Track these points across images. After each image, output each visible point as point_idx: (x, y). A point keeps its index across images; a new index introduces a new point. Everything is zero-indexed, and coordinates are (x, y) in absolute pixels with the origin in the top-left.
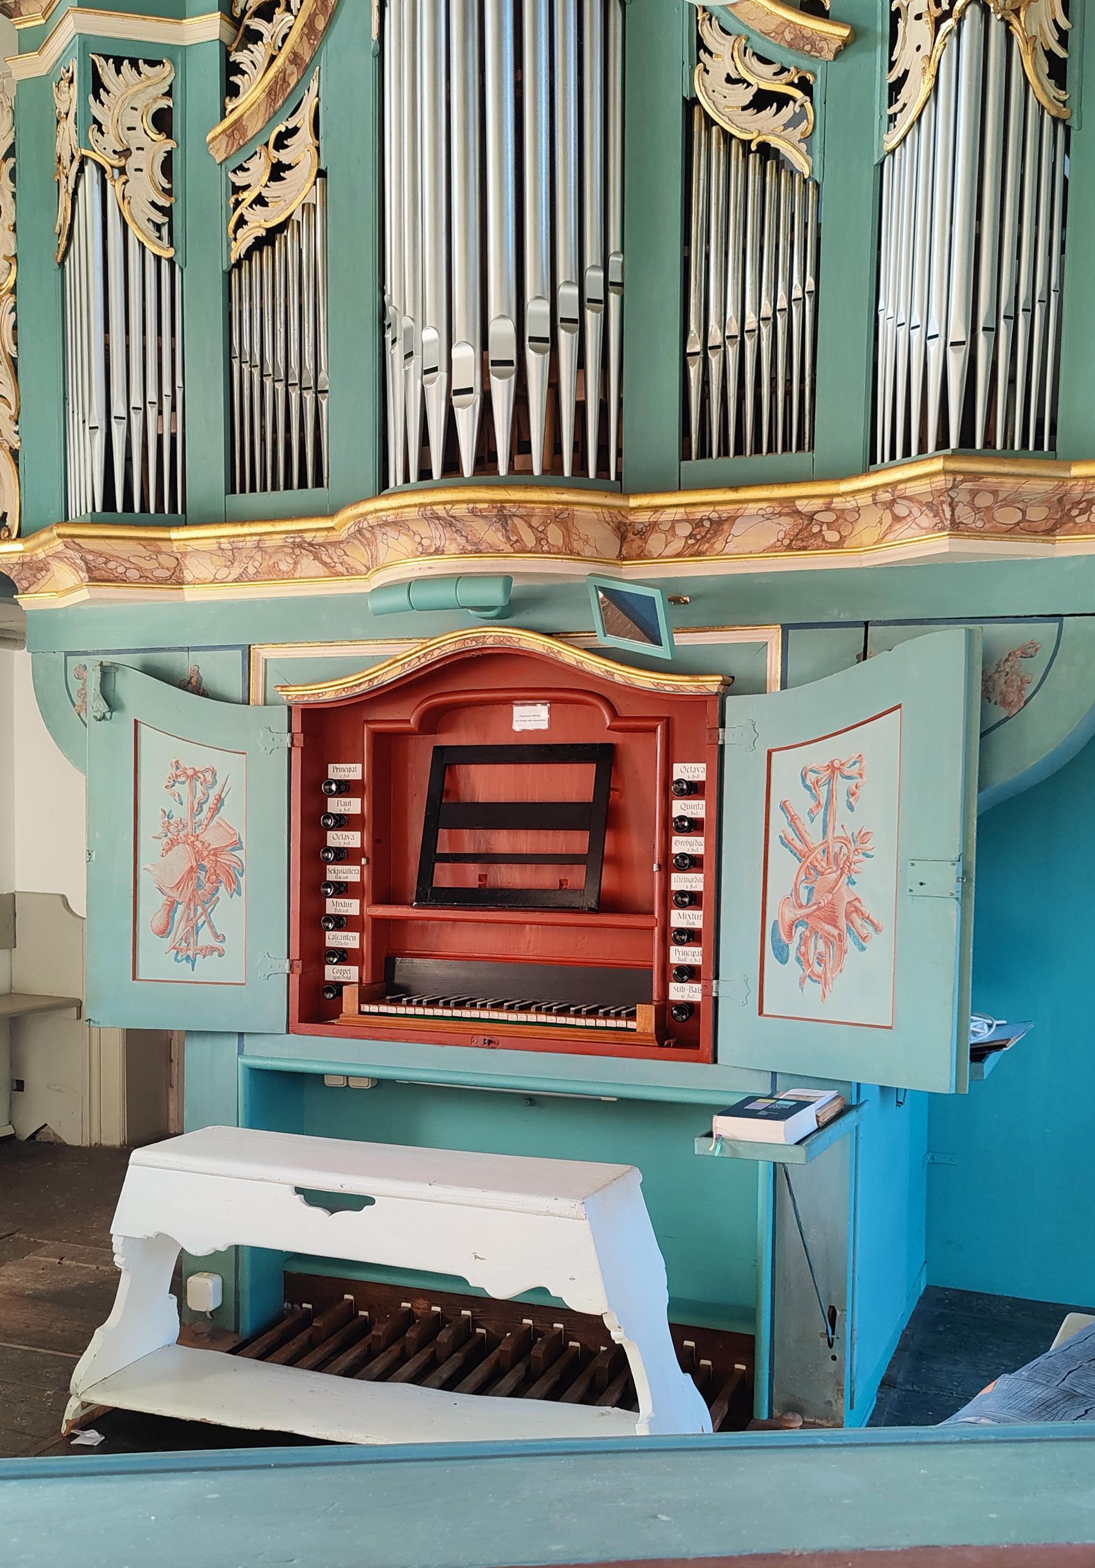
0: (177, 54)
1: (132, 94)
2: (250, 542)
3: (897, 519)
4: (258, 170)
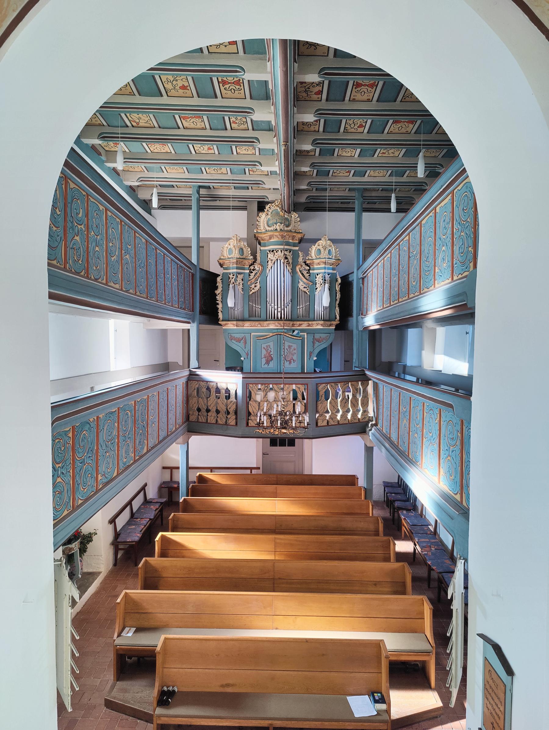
0: (244, 273)
1: (240, 277)
4: (253, 286)
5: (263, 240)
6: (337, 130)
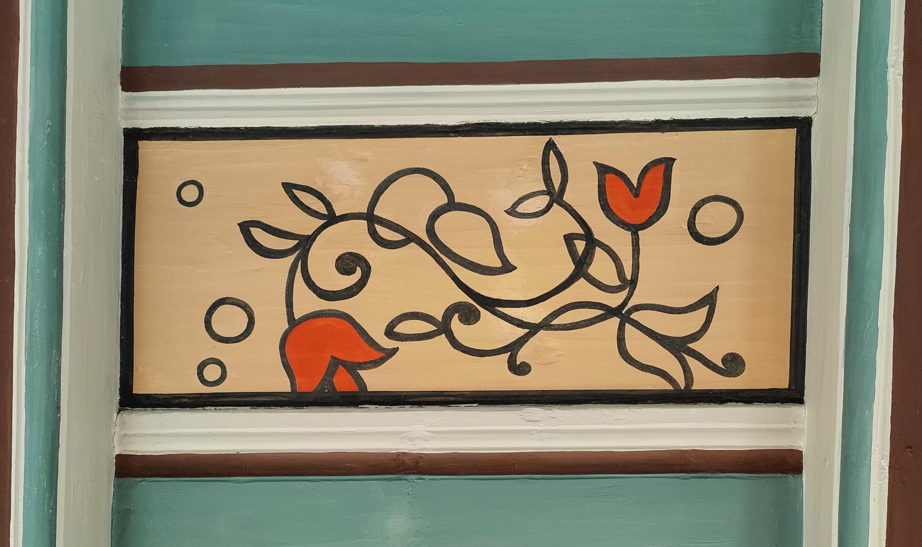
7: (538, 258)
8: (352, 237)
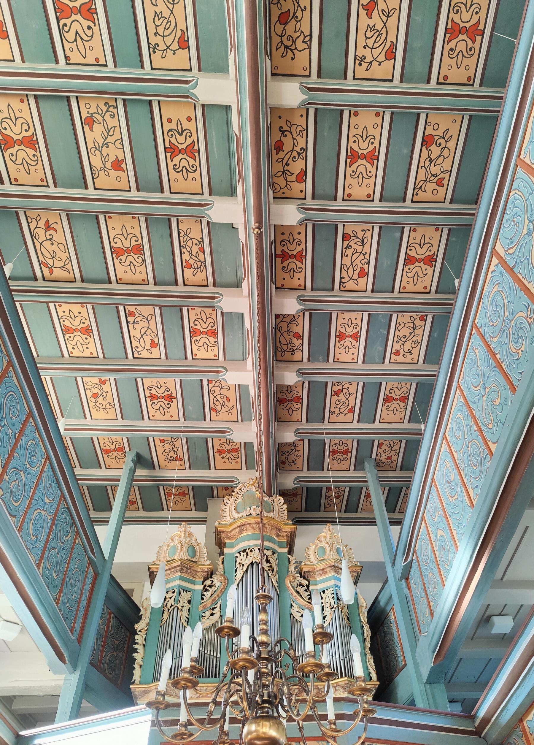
0: (193, 590)
1: (185, 596)
2: (205, 688)
3: (336, 690)
4: (208, 613)
5: (228, 538)
6: (330, 287)
7: (435, 170)
8: (443, 145)
